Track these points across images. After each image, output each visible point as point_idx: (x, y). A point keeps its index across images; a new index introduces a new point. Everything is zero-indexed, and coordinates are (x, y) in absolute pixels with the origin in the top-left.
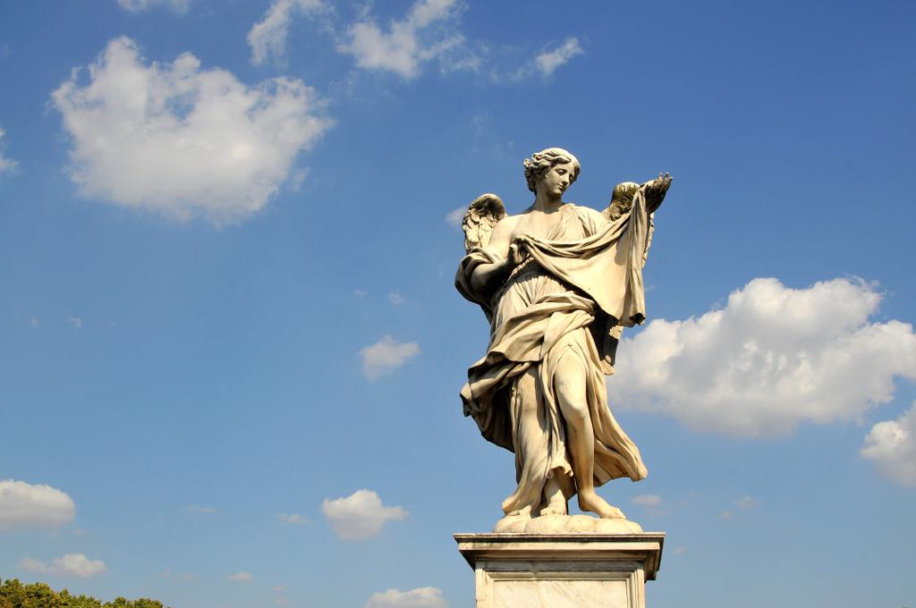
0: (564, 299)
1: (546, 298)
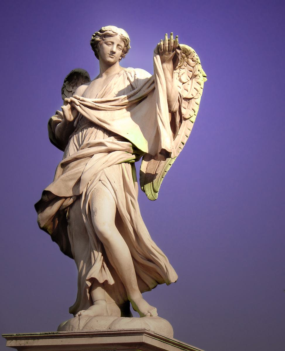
0: (101, 144)
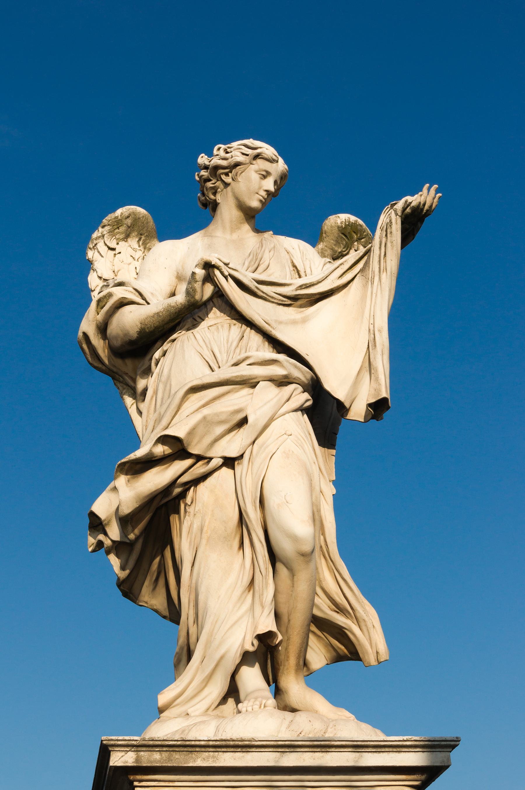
1: (247, 358)
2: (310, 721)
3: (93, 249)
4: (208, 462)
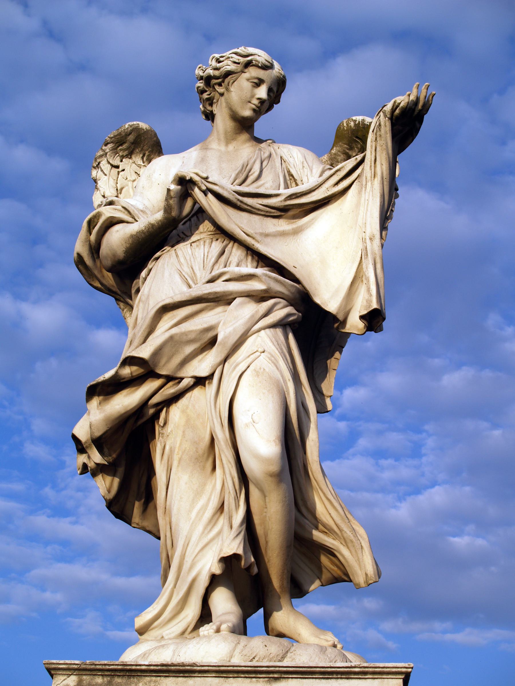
2: (266, 646)
3: (97, 168)
4: (179, 382)
